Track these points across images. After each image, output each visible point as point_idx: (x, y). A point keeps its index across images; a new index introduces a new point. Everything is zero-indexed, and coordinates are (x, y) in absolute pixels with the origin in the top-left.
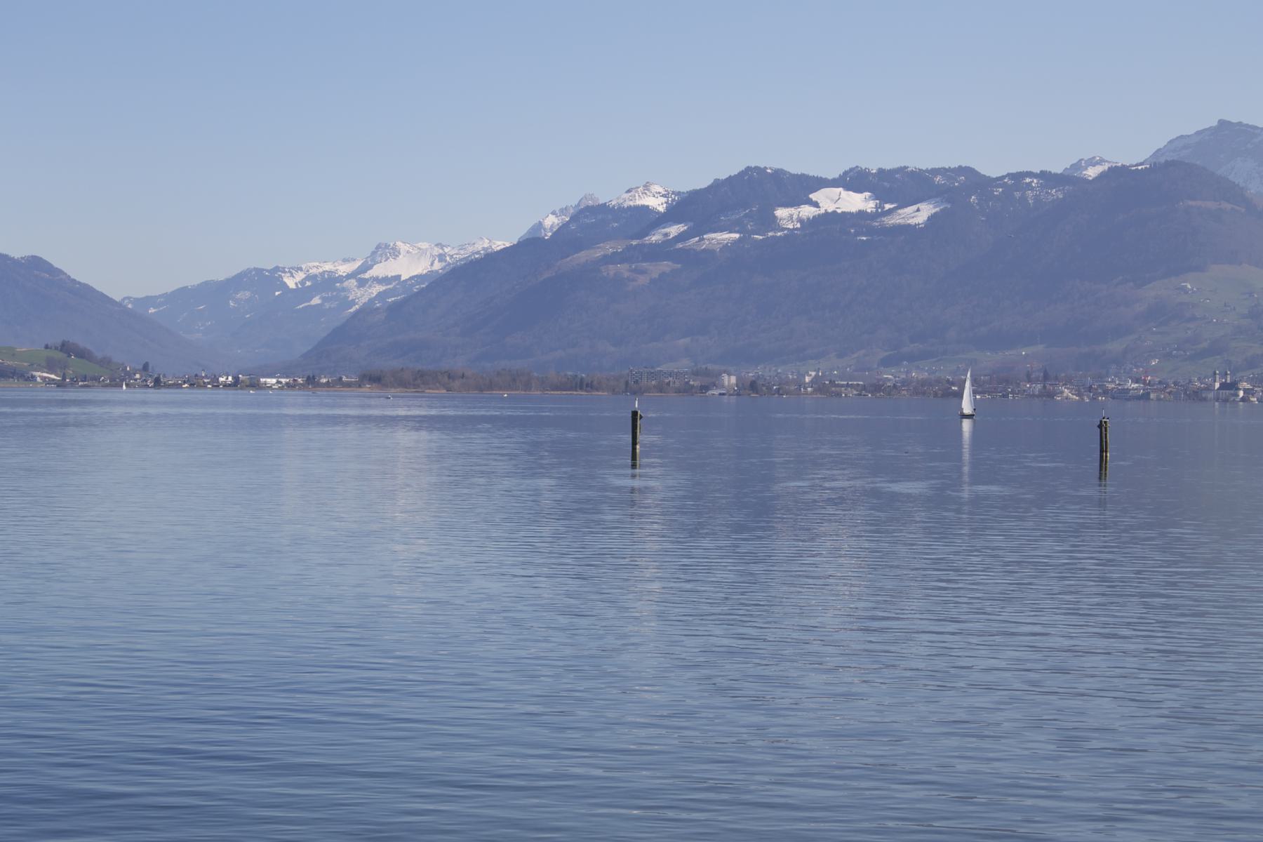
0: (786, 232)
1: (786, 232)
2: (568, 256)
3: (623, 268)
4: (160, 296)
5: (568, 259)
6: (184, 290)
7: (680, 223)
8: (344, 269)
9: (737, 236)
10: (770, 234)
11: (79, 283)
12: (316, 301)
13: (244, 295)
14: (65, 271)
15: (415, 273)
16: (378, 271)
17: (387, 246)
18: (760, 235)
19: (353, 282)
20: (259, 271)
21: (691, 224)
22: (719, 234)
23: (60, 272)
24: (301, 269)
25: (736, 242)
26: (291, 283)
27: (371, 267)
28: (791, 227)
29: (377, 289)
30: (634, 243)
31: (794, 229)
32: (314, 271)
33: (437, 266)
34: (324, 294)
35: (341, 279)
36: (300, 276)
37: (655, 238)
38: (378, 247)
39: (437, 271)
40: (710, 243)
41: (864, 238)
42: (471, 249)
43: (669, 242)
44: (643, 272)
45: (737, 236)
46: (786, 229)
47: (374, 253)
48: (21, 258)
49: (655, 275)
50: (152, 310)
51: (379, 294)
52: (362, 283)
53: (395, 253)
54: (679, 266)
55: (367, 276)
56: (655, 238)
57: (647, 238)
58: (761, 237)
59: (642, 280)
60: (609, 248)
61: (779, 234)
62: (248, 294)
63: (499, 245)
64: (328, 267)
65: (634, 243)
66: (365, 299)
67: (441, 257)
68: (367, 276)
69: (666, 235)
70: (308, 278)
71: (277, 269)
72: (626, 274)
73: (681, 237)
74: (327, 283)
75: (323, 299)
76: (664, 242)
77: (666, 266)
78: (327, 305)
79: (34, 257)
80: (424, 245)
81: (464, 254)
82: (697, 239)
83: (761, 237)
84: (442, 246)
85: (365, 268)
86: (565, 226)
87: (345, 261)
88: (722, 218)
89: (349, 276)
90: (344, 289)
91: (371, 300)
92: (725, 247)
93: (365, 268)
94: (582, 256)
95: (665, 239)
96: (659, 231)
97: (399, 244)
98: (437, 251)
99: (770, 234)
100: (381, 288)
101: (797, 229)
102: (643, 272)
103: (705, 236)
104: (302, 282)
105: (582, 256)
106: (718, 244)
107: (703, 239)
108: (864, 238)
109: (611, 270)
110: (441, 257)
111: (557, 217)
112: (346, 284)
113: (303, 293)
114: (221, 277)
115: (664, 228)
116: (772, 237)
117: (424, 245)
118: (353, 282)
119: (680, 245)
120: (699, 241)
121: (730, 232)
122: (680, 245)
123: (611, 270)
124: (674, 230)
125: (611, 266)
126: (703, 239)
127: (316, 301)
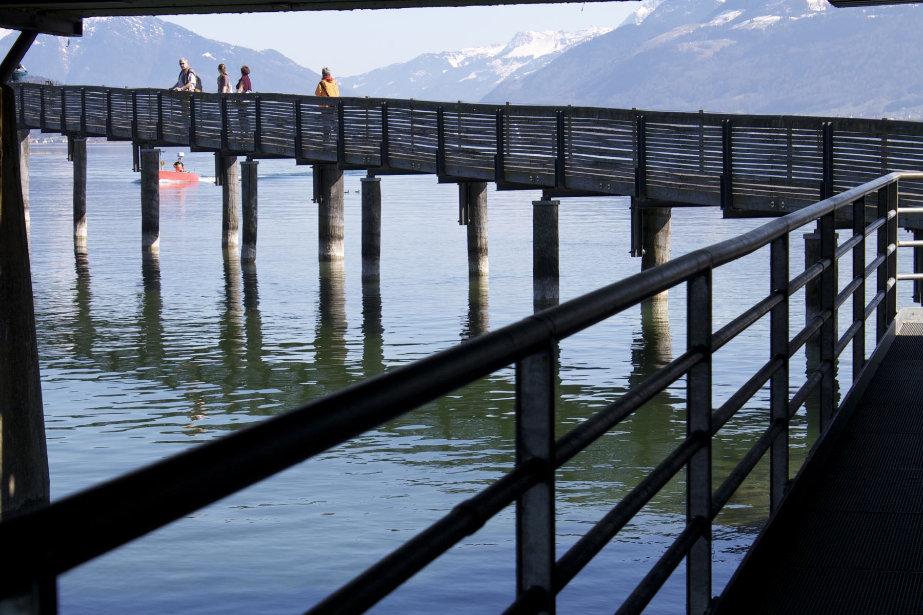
0: (815, 14)
1: (815, 14)
2: (653, 38)
3: (694, 45)
4: (360, 76)
5: (654, 39)
6: (377, 71)
7: (736, 10)
8: (492, 52)
9: (778, 18)
10: (803, 16)
11: (303, 68)
12: (472, 76)
13: (420, 73)
14: (293, 60)
15: (544, 53)
16: (517, 52)
17: (523, 34)
18: (796, 17)
19: (499, 61)
20: (431, 56)
21: (744, 10)
22: (765, 17)
23: (289, 60)
24: (461, 53)
25: (777, 23)
26: (454, 63)
27: (511, 50)
28: (819, 10)
29: (516, 66)
30: (702, 26)
31: (821, 12)
32: (470, 54)
33: (560, 48)
34: (478, 71)
35: (490, 60)
36: (461, 58)
37: (718, 21)
38: (517, 35)
39: (560, 51)
40: (758, 24)
41: (873, 16)
42: (584, 34)
43: (727, 25)
44: (708, 47)
45: (778, 18)
46: (815, 11)
47: (513, 39)
48: (262, 51)
49: (718, 49)
50: (355, 86)
51: (518, 70)
52: (506, 62)
53: (529, 39)
54: (735, 42)
55: (509, 56)
56: (718, 21)
57: (711, 22)
58: (796, 19)
59: (708, 53)
60: (683, 30)
61: (810, 15)
62: (423, 72)
63: (604, 30)
64: (481, 51)
65: (702, 26)
66: (507, 74)
67: (563, 41)
68: (509, 56)
69: (726, 19)
70: (466, 59)
71: (444, 53)
72: (696, 49)
73: (737, 20)
74: (480, 62)
75: (478, 75)
76: (723, 25)
77: (725, 42)
78: (480, 79)
79: (271, 51)
80: (550, 33)
81: (579, 38)
82: (749, 21)
83: (796, 19)
84: (562, 32)
85: (507, 51)
86: (652, 15)
87: (493, 46)
88: (767, 5)
89: (496, 57)
90: (492, 67)
91: (512, 75)
92: (770, 27)
93: (507, 51)
94: (664, 37)
95: (725, 22)
96: (721, 16)
97: (532, 32)
98: (560, 36)
99: (803, 16)
100: (519, 65)
101: (823, 11)
102: (708, 47)
103: (754, 19)
104: (463, 63)
105: (664, 37)
106: (764, 24)
107: (753, 21)
108: (873, 16)
109: (685, 47)
110: (563, 41)
111: (647, 8)
112: (494, 63)
113: (463, 70)
114: (404, 60)
115: (724, 14)
116: (805, 18)
117: (550, 33)
118: (499, 61)
119: (736, 27)
120: (751, 22)
121: (773, 15)
122: (736, 27)
123: (685, 47)
124: (732, 15)
125: (685, 44)
126: (753, 21)
127: (472, 76)
